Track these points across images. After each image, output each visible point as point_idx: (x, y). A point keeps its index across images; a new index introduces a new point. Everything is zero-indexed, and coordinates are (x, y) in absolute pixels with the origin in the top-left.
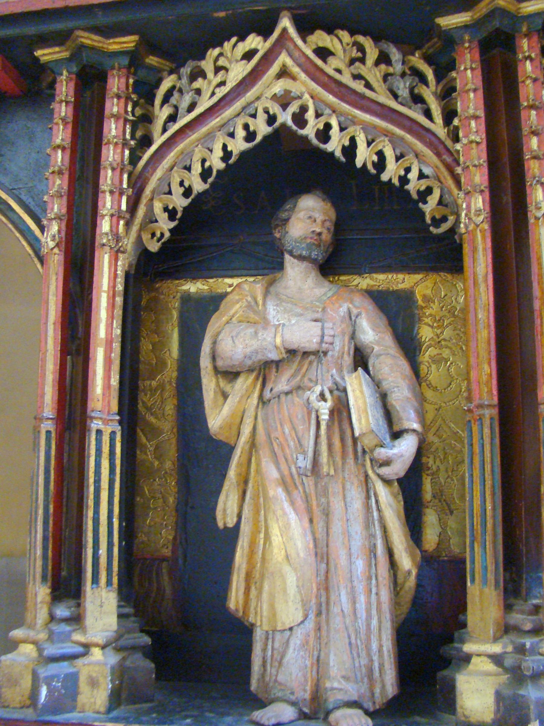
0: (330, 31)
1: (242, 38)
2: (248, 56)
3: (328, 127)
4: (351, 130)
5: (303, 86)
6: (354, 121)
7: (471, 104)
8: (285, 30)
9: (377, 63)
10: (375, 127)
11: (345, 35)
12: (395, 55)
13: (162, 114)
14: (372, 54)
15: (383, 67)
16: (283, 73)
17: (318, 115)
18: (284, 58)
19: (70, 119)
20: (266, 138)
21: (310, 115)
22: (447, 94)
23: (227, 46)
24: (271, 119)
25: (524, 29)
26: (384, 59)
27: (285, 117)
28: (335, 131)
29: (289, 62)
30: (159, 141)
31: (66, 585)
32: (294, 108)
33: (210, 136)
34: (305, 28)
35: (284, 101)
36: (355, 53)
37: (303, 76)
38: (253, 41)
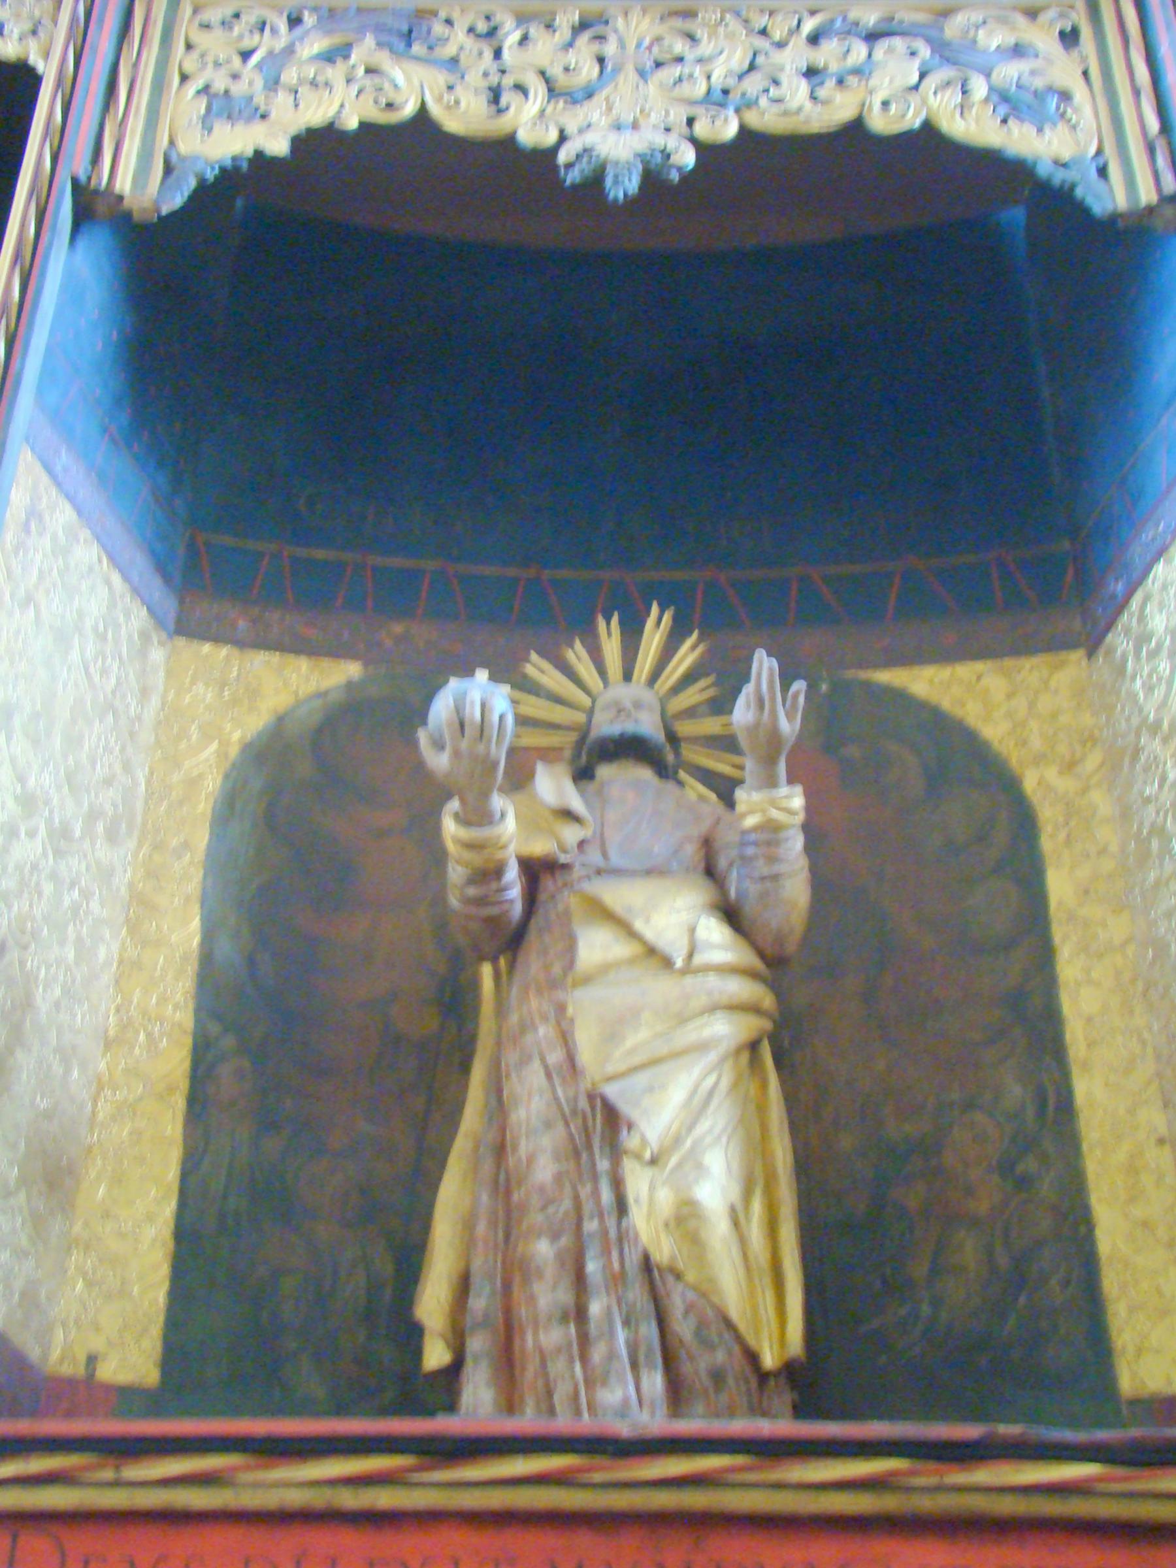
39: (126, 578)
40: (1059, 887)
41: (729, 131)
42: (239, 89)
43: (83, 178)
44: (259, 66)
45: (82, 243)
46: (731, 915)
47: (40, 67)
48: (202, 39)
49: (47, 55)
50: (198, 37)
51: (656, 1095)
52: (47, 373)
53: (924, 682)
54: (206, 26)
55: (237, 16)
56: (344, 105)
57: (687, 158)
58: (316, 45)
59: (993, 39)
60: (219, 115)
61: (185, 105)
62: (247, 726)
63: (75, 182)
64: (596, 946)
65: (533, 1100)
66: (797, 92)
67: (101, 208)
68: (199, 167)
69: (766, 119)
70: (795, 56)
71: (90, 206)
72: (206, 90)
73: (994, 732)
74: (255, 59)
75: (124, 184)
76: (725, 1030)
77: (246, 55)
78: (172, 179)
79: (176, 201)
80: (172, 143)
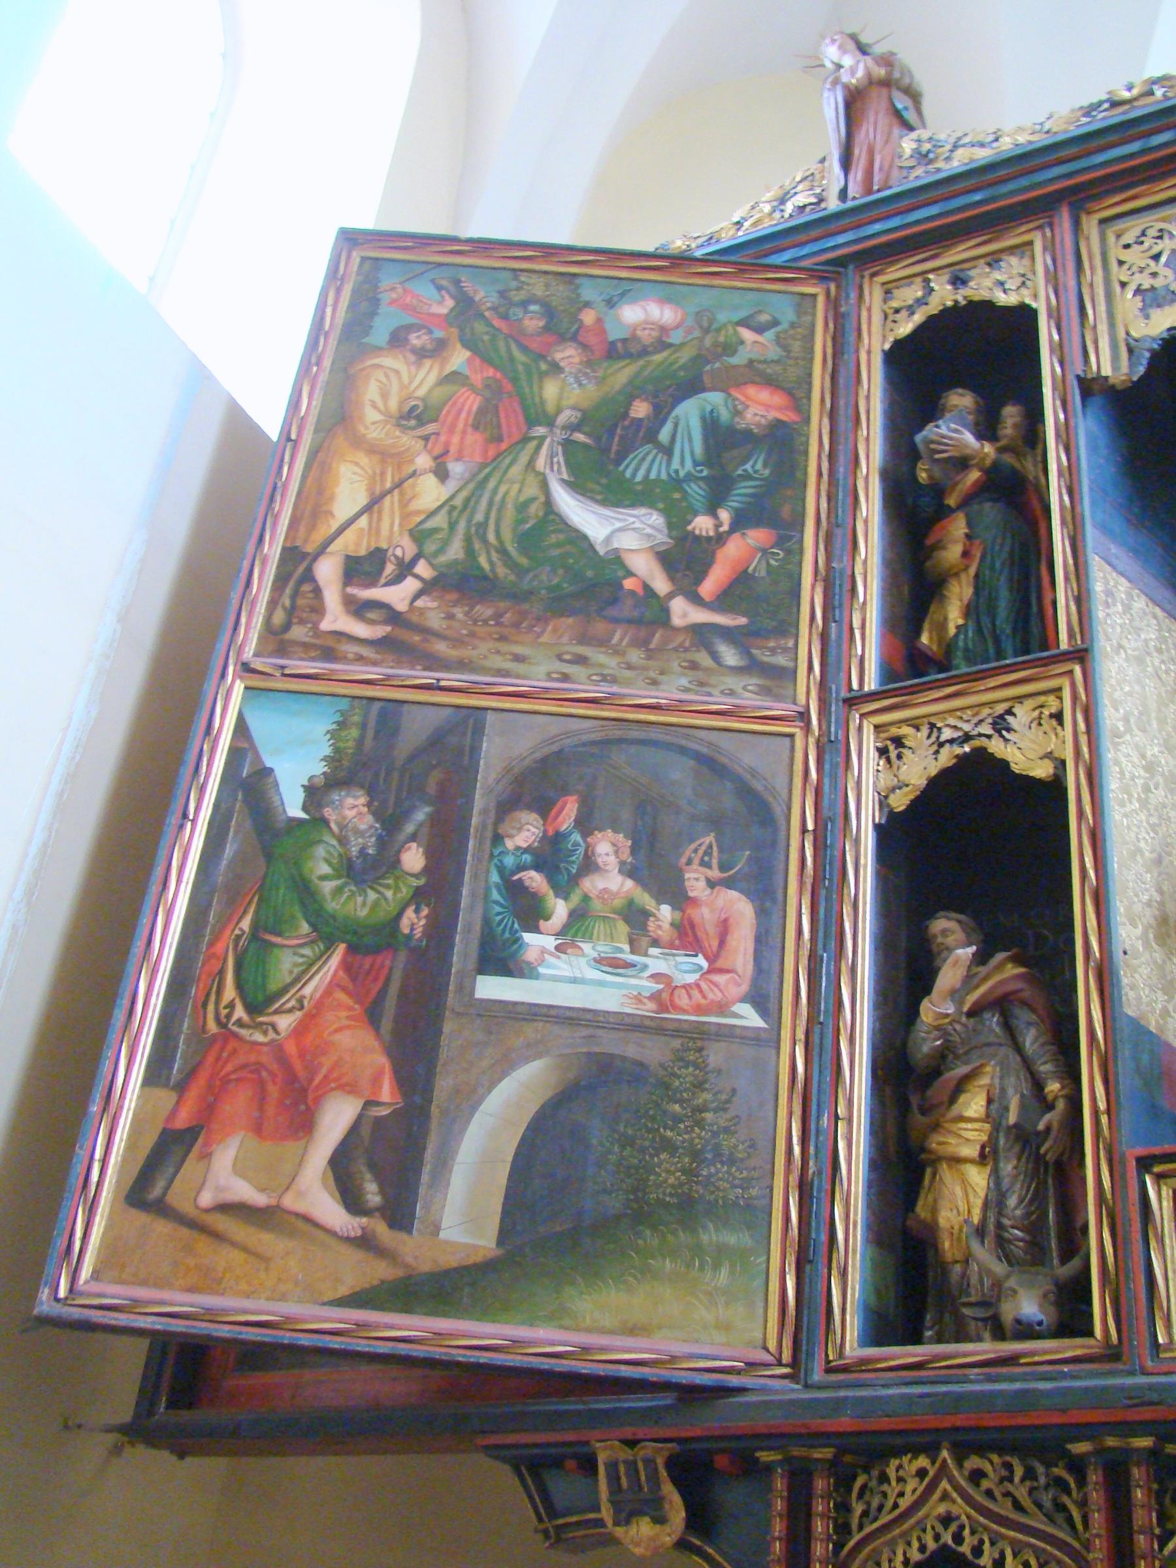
0: (982, 1456)
1: (915, 1457)
2: (922, 1473)
3: (982, 1542)
4: (1000, 1545)
5: (959, 1507)
6: (1003, 1537)
7: (1098, 1518)
8: (944, 1461)
9: (1023, 1480)
10: (1020, 1541)
11: (995, 1458)
12: (1040, 1469)
13: (858, 1508)
14: (1019, 1472)
15: (1028, 1483)
16: (945, 1497)
17: (973, 1532)
18: (944, 1484)
19: (784, 1513)
20: (933, 1553)
21: (967, 1532)
22: (1083, 1504)
23: (905, 1459)
24: (937, 1537)
25: (1135, 1459)
26: (1030, 1474)
27: (947, 1538)
28: (987, 1545)
29: (949, 1487)
30: (857, 1537)
32: (953, 1527)
33: (892, 1544)
34: (961, 1451)
35: (946, 1520)
36: (1004, 1473)
37: (959, 1500)
38: (922, 1461)
39: (1163, 609)
42: (1158, 283)
43: (1082, 375)
44: (1167, 265)
45: (1089, 410)
47: (1034, 305)
48: (1125, 255)
49: (1035, 297)
50: (1125, 255)
52: (1093, 503)
54: (1127, 246)
55: (1143, 234)
60: (1151, 306)
63: (1078, 377)
67: (1096, 388)
68: (1147, 345)
71: (1089, 387)
72: (1138, 291)
74: (1163, 259)
75: (1106, 371)
77: (1156, 257)
78: (1134, 359)
79: (1141, 370)
80: (1128, 334)
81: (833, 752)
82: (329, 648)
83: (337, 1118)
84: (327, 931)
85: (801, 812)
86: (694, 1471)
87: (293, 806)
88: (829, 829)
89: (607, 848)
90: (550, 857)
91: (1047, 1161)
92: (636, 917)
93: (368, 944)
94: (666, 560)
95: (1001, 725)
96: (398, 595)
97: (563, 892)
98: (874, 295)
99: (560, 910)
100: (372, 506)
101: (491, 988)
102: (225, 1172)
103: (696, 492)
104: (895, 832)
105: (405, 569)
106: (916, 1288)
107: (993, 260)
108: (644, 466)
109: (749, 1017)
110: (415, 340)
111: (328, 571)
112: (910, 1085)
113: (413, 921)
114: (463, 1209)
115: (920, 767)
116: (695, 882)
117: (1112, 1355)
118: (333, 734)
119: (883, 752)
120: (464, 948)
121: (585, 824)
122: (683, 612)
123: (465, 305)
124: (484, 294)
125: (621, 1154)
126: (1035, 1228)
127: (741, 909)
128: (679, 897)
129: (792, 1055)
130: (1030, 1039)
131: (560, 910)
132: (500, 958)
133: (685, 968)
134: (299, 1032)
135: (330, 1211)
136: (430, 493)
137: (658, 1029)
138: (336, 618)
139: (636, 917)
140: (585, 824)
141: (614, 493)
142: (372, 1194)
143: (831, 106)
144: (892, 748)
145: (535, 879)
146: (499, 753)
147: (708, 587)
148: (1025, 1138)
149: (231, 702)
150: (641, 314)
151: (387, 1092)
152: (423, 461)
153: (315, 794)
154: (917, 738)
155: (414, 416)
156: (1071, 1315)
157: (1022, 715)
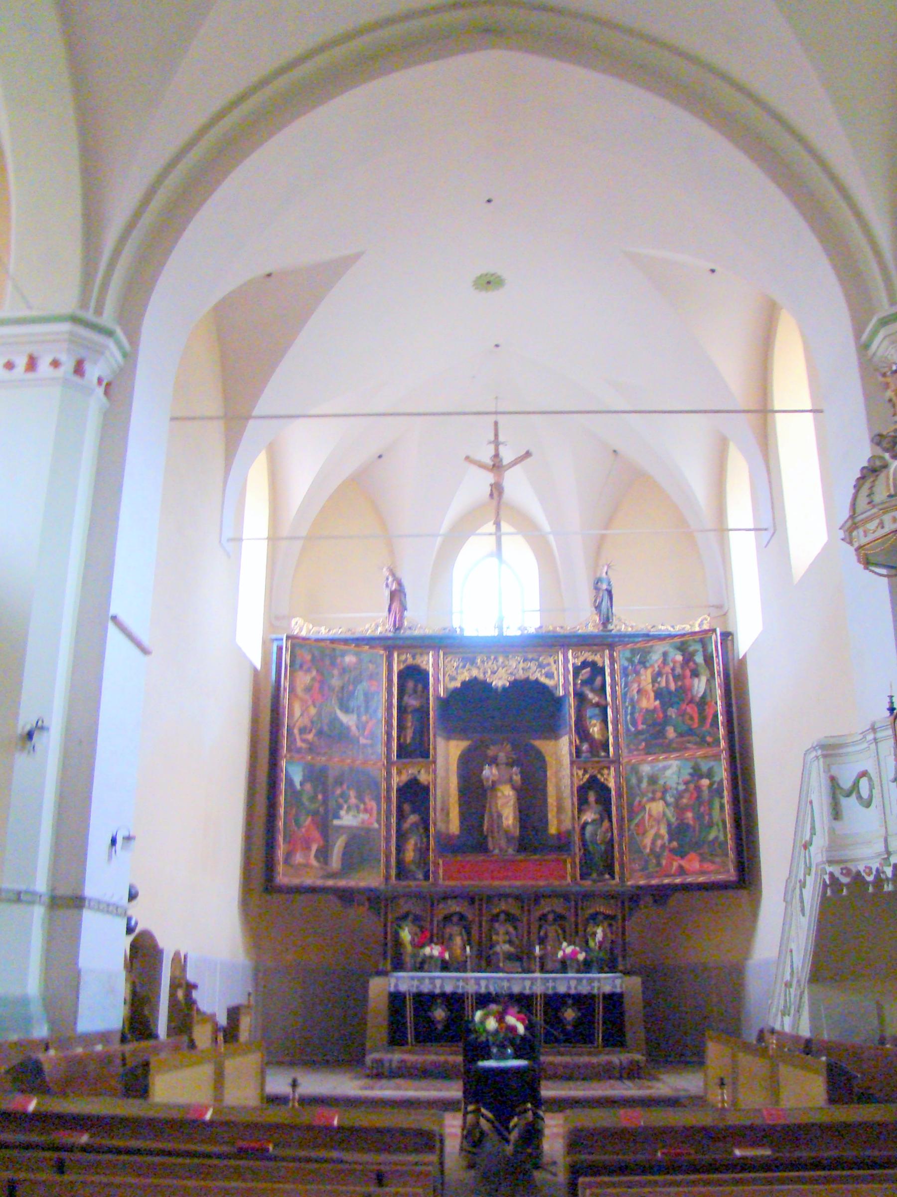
31: (385, 959)
40: (549, 773)
41: (512, 678)
46: (514, 788)
51: (506, 807)
53: (538, 743)
56: (465, 676)
57: (508, 684)
58: (461, 665)
59: (545, 662)
61: (447, 678)
62: (459, 753)
64: (499, 794)
65: (494, 810)
66: (521, 672)
69: (518, 677)
70: (521, 665)
73: (543, 750)
76: (512, 802)
81: (389, 773)
82: (299, 751)
83: (314, 847)
84: (308, 813)
85: (384, 785)
86: (369, 899)
87: (298, 787)
88: (389, 788)
89: (352, 793)
90: (342, 795)
91: (423, 852)
92: (357, 807)
93: (315, 813)
94: (358, 728)
95: (419, 772)
96: (310, 737)
97: (346, 802)
98: (396, 655)
99: (345, 807)
100: (302, 715)
101: (336, 822)
102: (299, 858)
103: (362, 709)
104: (398, 790)
105: (311, 731)
106: (402, 871)
107: (421, 654)
108: (352, 704)
109: (376, 825)
110: (305, 668)
111: (296, 731)
112: (402, 837)
113: (321, 810)
114: (335, 862)
115: (405, 778)
116: (367, 800)
117: (432, 884)
118: (303, 771)
119: (397, 773)
120: (330, 816)
121: (348, 788)
122: (362, 741)
123: (313, 656)
124: (316, 653)
125: (358, 850)
126: (420, 863)
127: (373, 804)
128: (365, 804)
129: (383, 833)
130: (421, 831)
131: (345, 807)
132: (338, 817)
133: (366, 816)
134: (307, 831)
135: (314, 863)
136: (313, 711)
137: (362, 829)
138: (299, 744)
139: (357, 807)
140: (348, 788)
141: (346, 710)
142: (322, 859)
143: (387, 593)
144: (399, 773)
145: (341, 800)
146: (332, 774)
147: (366, 733)
148: (420, 850)
149: (283, 763)
150: (350, 659)
151: (322, 843)
152: (310, 702)
153: (301, 784)
154: (404, 772)
155: (308, 689)
156: (427, 877)
157: (423, 771)
